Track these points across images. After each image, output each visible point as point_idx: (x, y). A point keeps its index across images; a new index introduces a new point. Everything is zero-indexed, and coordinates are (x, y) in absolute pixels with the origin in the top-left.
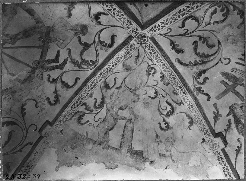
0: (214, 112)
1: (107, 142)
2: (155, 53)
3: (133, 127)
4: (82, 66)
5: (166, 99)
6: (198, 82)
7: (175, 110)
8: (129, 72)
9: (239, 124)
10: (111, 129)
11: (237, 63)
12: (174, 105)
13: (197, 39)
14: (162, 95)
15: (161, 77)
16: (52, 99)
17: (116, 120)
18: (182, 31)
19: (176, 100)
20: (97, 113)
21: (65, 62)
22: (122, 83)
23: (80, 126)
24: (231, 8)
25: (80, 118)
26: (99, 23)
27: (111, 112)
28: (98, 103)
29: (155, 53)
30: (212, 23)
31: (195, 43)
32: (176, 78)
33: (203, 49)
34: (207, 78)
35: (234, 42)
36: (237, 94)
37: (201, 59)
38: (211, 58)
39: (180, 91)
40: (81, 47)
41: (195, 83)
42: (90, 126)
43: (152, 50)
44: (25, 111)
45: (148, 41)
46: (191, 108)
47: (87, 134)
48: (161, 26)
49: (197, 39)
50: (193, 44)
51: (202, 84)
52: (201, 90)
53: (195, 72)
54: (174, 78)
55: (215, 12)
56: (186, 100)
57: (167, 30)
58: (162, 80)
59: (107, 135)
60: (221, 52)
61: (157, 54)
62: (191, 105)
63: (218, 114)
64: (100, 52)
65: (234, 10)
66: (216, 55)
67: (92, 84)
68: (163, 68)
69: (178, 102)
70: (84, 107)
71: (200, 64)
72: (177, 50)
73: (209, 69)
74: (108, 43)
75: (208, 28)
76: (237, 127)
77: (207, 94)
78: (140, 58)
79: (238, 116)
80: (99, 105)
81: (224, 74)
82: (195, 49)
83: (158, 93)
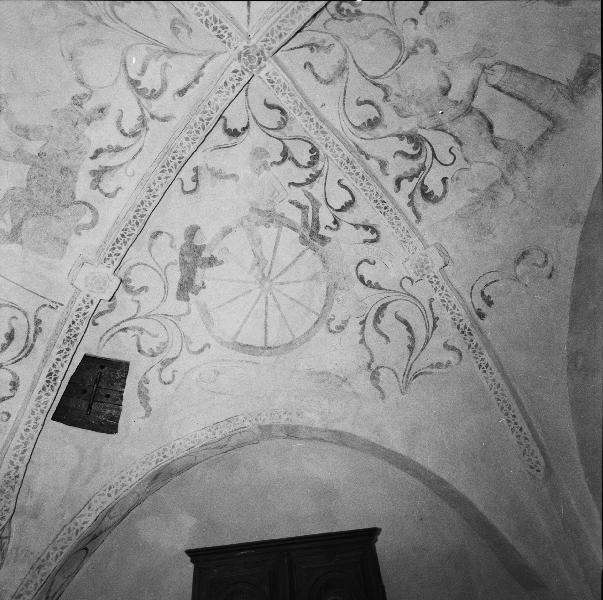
1: (520, 148)
2: (279, 27)
3: (507, 65)
4: (319, 169)
8: (351, 65)
10: (490, 127)
16: (368, 235)
17: (469, 110)
20: (434, 155)
21: (309, 195)
22: (375, 84)
23: (446, 202)
25: (427, 196)
26: (244, 129)
27: (445, 119)
28: (409, 149)
29: (279, 27)
40: (289, 163)
42: (457, 179)
44: (373, 283)
45: (255, 46)
47: (473, 190)
59: (502, 142)
64: (296, 132)
70: (404, 183)
74: (280, 115)
78: (317, 41)
80: (415, 148)
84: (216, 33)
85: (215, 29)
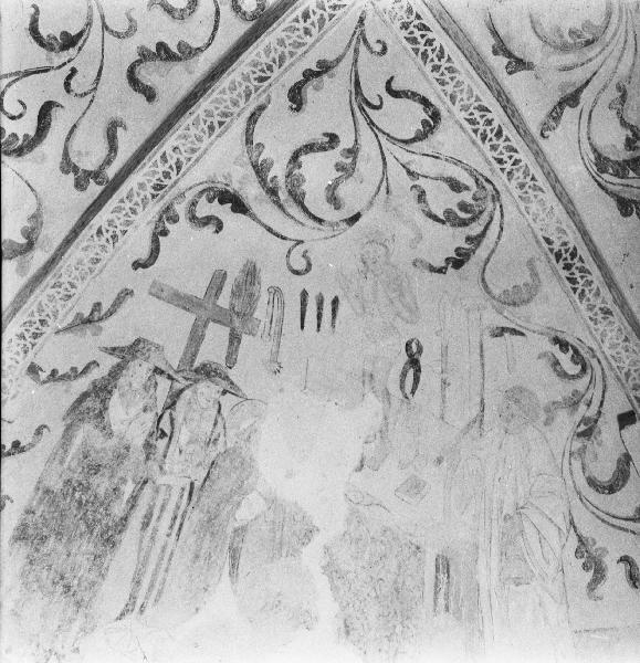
0: (98, 305)
2: (307, 32)
5: (58, 94)
6: (194, 204)
7: (28, 156)
9: (97, 396)
11: (304, 294)
12: (52, 145)
13: (346, 142)
14: (74, 71)
15: (161, 46)
18: (374, 89)
19: (75, 145)
24: (475, 229)
29: (307, 32)
30: (416, 183)
31: (333, 139)
32: (213, 137)
33: (317, 172)
34: (220, 227)
35: (369, 262)
36: (196, 338)
37: (281, 181)
38: (294, 210)
39: (162, 168)
41: (190, 196)
43: (322, 20)
46: (103, 239)
48: (429, 48)
49: (346, 142)
50: (326, 135)
51: (193, 218)
52: (167, 224)
53: (228, 176)
54: (211, 128)
55: (456, 186)
56: (128, 205)
57: (379, 41)
58: (144, 56)
60: (323, 234)
61: (304, 44)
62: (118, 233)
63: (100, 319)
65: (468, 239)
66: (311, 223)
67: (431, 45)
68: (246, 78)
69: (74, 159)
71: (263, 181)
72: (300, 89)
73: (259, 222)
75: (397, 175)
76: (85, 395)
77: (155, 252)
79: (122, 381)
81: (251, 273)
82: (310, 148)
83: (72, 51)
84: (430, 36)
85: (429, 42)
